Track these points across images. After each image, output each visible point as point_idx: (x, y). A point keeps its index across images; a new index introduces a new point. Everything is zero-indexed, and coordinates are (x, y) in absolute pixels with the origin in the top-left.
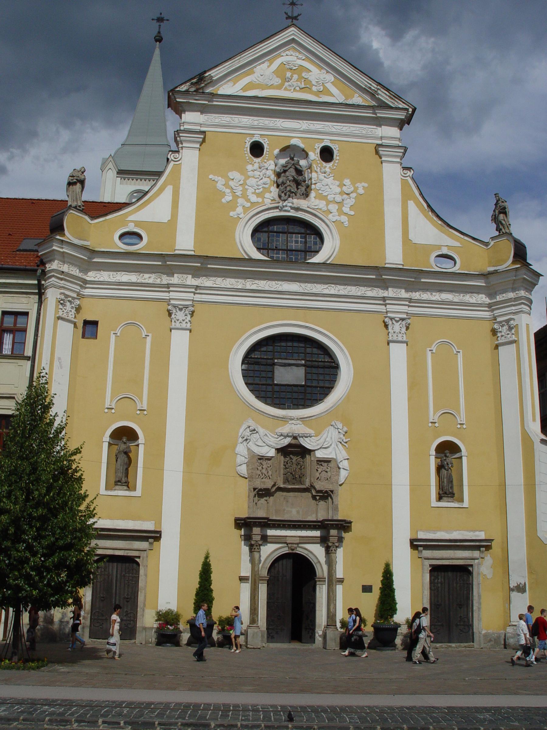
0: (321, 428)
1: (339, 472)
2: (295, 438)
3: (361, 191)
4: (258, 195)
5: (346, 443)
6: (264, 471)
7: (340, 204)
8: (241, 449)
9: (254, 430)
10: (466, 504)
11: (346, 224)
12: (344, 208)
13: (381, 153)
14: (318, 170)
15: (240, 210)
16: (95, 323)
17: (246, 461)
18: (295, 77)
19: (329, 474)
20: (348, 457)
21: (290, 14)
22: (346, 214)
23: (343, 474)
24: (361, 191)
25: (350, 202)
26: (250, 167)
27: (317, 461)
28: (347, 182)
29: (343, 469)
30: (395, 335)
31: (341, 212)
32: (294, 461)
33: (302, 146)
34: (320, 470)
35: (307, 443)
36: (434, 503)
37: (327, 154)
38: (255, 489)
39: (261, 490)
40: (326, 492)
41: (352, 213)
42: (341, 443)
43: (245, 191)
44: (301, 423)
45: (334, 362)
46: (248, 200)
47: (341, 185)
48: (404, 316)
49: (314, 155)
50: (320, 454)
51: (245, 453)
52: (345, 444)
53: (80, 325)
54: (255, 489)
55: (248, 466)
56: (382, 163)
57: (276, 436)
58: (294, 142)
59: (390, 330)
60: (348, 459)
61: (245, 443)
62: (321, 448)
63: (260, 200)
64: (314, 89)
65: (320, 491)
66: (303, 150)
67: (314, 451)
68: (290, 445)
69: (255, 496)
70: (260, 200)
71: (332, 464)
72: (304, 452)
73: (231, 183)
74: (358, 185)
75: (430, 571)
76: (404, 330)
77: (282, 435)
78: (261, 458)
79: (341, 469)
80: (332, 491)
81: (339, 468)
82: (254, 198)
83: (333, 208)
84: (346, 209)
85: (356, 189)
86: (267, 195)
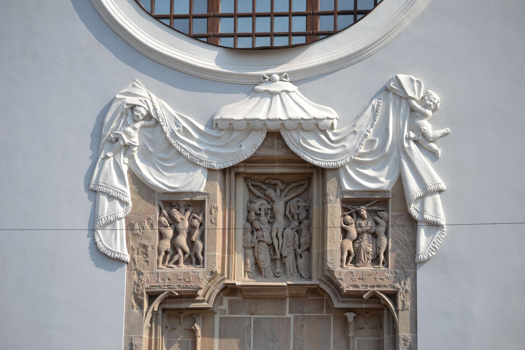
2: (274, 135)
32: (279, 207)
35: (315, 150)
39: (171, 297)
40: (374, 297)
54: (152, 297)
55: (130, 227)
65: (357, 296)
67: (336, 170)
71: (392, 213)
72: (308, 177)
78: (171, 202)
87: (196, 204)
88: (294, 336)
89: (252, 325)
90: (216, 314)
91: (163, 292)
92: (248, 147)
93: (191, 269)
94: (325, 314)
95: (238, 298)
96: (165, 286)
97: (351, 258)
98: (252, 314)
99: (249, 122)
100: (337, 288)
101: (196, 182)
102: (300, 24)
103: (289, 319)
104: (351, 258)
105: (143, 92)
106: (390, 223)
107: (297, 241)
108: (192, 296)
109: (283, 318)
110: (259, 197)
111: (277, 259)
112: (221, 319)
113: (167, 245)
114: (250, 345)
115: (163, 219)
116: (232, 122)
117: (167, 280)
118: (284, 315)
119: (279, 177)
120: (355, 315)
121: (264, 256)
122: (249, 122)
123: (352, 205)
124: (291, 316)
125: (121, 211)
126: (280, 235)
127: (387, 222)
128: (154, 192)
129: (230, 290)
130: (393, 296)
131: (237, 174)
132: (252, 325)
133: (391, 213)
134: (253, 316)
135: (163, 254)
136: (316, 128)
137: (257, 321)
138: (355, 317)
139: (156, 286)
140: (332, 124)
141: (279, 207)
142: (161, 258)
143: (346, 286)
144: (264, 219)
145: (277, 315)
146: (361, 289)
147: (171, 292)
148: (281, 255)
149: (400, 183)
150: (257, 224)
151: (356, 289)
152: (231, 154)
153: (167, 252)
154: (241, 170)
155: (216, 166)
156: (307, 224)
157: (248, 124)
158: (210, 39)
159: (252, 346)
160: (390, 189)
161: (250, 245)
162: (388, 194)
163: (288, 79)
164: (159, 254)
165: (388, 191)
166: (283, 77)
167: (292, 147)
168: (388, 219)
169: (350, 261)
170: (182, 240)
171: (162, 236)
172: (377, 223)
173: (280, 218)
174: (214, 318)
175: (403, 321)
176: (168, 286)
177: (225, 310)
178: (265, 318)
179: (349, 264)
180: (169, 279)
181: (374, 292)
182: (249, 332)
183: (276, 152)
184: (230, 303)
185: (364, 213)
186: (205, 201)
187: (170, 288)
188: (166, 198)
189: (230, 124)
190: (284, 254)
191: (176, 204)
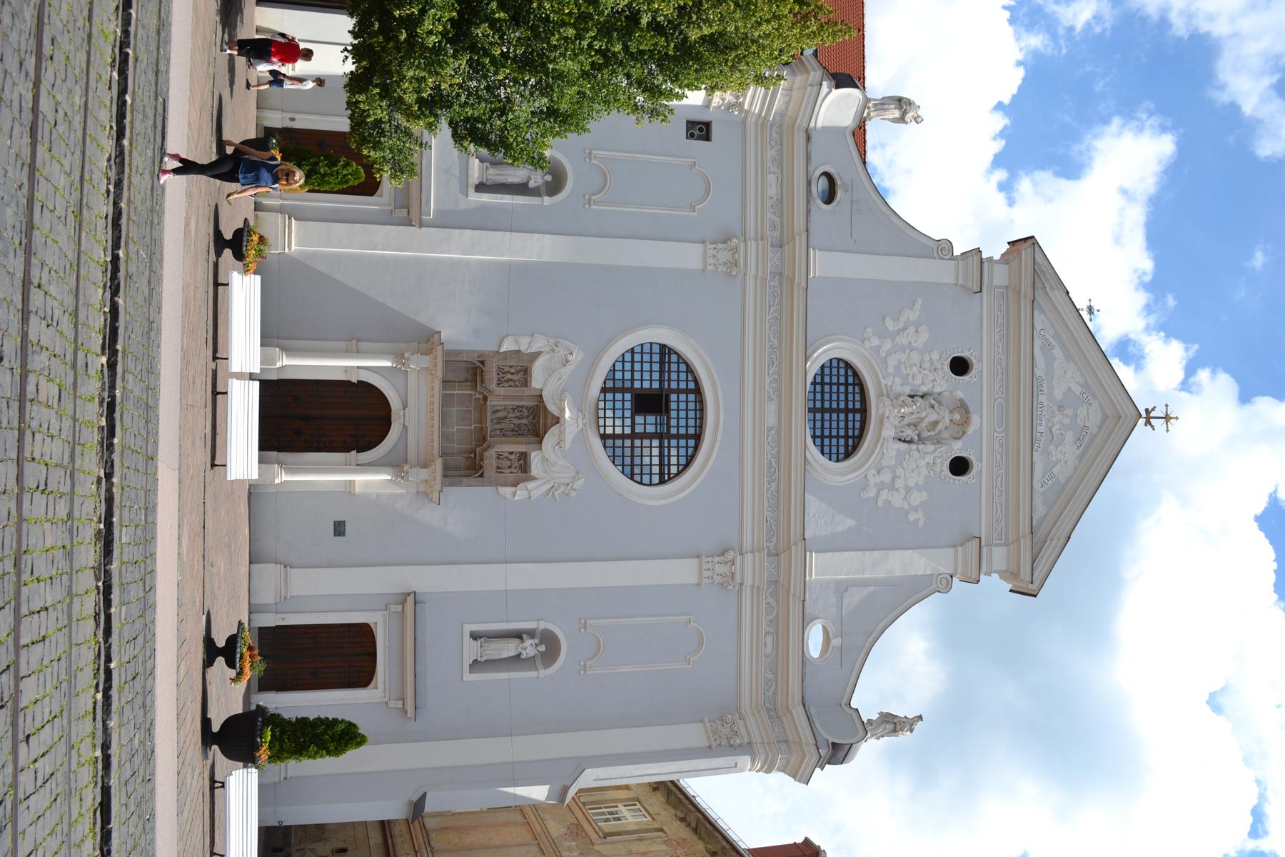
0: (573, 452)
3: (912, 517)
4: (897, 367)
7: (892, 487)
8: (539, 344)
10: (468, 677)
11: (865, 495)
12: (886, 491)
13: (969, 544)
14: (937, 454)
15: (875, 342)
16: (707, 137)
18: (1067, 421)
19: (508, 471)
21: (1152, 414)
22: (878, 495)
23: (506, 491)
24: (912, 517)
25: (897, 500)
26: (935, 355)
28: (924, 496)
30: (710, 566)
31: (880, 487)
32: (524, 421)
33: (970, 431)
34: (512, 457)
35: (549, 440)
36: (469, 628)
37: (960, 466)
38: (482, 362)
39: (482, 371)
40: (481, 467)
41: (880, 503)
43: (903, 349)
45: (670, 478)
46: (889, 354)
47: (919, 488)
48: (738, 579)
49: (958, 449)
50: (535, 458)
53: (704, 117)
54: (482, 362)
56: (954, 546)
58: (975, 419)
59: (717, 559)
63: (891, 370)
64: (1052, 448)
66: (964, 433)
70: (891, 370)
73: (912, 329)
74: (920, 515)
75: (367, 625)
76: (717, 579)
78: (526, 371)
80: (481, 476)
82: (892, 362)
83: (886, 477)
84: (885, 494)
85: (916, 509)
86: (898, 381)
87: (526, 383)
92: (552, 408)
93: (495, 382)
100: (485, 450)
101: (536, 382)
102: (609, 431)
105: (579, 358)
108: (482, 382)
111: (500, 420)
113: (507, 369)
119: (537, 421)
121: (501, 414)
123: (524, 457)
125: (523, 348)
129: (485, 399)
130: (481, 476)
141: (524, 421)
143: (486, 454)
149: (534, 479)
156: (517, 432)
158: (604, 390)
170: (509, 376)
175: (470, 480)
183: (549, 421)
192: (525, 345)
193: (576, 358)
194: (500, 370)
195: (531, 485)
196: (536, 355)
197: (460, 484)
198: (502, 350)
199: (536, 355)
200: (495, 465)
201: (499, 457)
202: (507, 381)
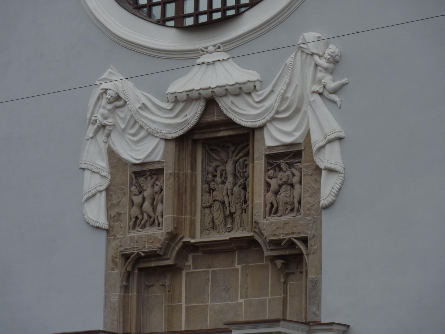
1: (318, 181)
5: (335, 91)
6: (147, 206)
9: (118, 98)
17: (105, 184)
20: (342, 135)
23: (328, 187)
27: (269, 157)
29: (331, 171)
34: (274, 183)
35: (244, 113)
39: (139, 259)
40: (291, 244)
42: (321, 94)
44: (223, 56)
50: (277, 136)
51: (103, 164)
52: (334, 97)
55: (108, 198)
57: (169, 106)
60: (340, 139)
61: (101, 137)
62: (273, 119)
67: (261, 128)
68: (199, 127)
69: (128, 275)
72: (243, 138)
77: (176, 101)
79: (324, 173)
80: (305, 241)
81: (318, 170)
88: (241, 285)
89: (210, 277)
90: (183, 269)
91: (133, 253)
94: (264, 263)
95: (199, 254)
96: (134, 248)
97: (274, 209)
98: (210, 267)
99: (188, 93)
103: (238, 270)
104: (274, 209)
106: (303, 173)
107: (243, 197)
109: (233, 270)
110: (216, 160)
112: (187, 274)
113: (135, 211)
114: (208, 295)
115: (133, 188)
116: (176, 94)
117: (135, 244)
118: (234, 266)
120: (283, 261)
121: (218, 215)
122: (188, 93)
124: (239, 267)
126: (229, 193)
127: (301, 173)
128: (126, 164)
131: (195, 142)
132: (210, 277)
133: (303, 164)
134: (210, 270)
135: (133, 220)
136: (241, 91)
137: (214, 273)
138: (283, 264)
139: (127, 249)
140: (255, 87)
141: (229, 167)
142: (132, 223)
144: (218, 179)
145: (228, 267)
146: (281, 237)
147: (138, 254)
148: (230, 211)
150: (212, 185)
151: (276, 238)
152: (180, 124)
153: (137, 218)
154: (196, 137)
155: (170, 136)
157: (188, 95)
159: (209, 297)
160: (301, 141)
161: (208, 204)
162: (301, 146)
163: (222, 49)
164: (130, 219)
165: (301, 144)
166: (218, 48)
167: (225, 111)
168: (301, 169)
169: (273, 213)
171: (132, 203)
172: (294, 175)
173: (230, 179)
174: (181, 273)
176: (136, 248)
177: (190, 265)
178: (219, 270)
179: (272, 215)
180: (137, 242)
181: (290, 240)
182: (208, 284)
184: (194, 258)
185: (283, 166)
186: (163, 168)
187: (138, 250)
188: (136, 169)
189: (176, 97)
190: (233, 210)
191: (144, 174)
192: (95, 182)
193: (114, 81)
194: (137, 223)
195: (317, 139)
196: (113, 156)
197: (316, 284)
198: (103, 221)
199: (113, 156)
200: (288, 217)
201: (273, 210)
202: (154, 208)
